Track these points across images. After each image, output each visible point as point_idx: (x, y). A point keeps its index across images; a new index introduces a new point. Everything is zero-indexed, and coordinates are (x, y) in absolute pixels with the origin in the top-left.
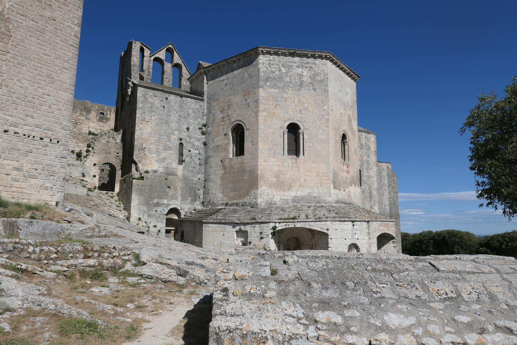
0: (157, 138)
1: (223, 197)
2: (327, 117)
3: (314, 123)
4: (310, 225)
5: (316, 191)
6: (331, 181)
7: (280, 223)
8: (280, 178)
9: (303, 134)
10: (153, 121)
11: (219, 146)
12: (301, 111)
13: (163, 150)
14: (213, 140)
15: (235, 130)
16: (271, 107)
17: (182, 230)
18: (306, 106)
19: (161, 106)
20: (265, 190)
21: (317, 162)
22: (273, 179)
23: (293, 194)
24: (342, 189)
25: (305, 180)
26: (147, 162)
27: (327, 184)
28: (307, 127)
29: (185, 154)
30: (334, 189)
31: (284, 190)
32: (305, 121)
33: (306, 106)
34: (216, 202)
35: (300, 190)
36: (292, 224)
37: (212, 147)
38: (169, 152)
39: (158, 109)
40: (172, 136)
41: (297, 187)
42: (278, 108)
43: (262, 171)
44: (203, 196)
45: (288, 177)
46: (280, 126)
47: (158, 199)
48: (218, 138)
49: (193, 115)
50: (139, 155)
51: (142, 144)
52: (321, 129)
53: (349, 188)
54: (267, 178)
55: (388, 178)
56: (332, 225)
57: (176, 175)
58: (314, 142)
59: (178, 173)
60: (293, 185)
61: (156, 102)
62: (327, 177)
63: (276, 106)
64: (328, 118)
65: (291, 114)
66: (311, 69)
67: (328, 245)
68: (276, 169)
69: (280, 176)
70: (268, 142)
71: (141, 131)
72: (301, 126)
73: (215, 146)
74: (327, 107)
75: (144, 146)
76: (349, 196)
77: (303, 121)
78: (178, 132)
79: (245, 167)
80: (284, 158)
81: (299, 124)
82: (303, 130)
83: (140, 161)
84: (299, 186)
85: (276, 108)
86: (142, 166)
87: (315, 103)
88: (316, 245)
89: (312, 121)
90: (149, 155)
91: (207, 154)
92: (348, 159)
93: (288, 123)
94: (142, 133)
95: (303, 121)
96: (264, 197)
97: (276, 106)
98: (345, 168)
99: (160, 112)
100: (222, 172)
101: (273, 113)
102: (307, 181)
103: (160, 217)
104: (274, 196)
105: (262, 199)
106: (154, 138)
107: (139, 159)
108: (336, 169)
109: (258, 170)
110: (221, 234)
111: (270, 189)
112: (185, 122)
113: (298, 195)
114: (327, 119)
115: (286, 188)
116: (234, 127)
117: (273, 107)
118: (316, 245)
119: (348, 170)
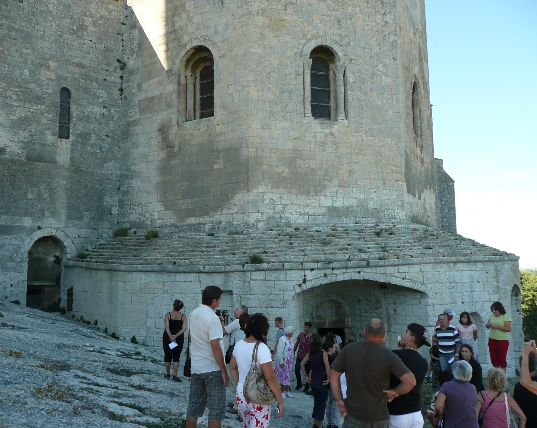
0: (5, 72)
1: (166, 212)
2: (392, 38)
3: (368, 50)
4: (385, 274)
5: (374, 196)
6: (403, 175)
7: (312, 270)
8: (299, 167)
9: (345, 71)
11: (153, 98)
12: (339, 21)
13: (18, 100)
14: (139, 86)
15: (191, 63)
16: (275, 7)
17: (68, 287)
18: (350, 11)
20: (264, 193)
21: (374, 134)
22: (282, 168)
23: (327, 202)
24: (417, 195)
25: (351, 173)
27: (396, 181)
28: (353, 57)
29: (74, 115)
30: (408, 192)
31: (308, 193)
32: (348, 44)
33: (350, 11)
34: (149, 222)
35: (341, 193)
36: (344, 273)
37: (139, 101)
38: (34, 107)
40: (43, 72)
41: (336, 188)
42: (290, 10)
43: (256, 150)
44: (118, 210)
45: (314, 164)
46: (295, 50)
47: (8, 215)
48: (151, 81)
49: (93, 29)
52: (382, 64)
53: (424, 193)
54: (270, 165)
55: (440, 185)
56: (433, 273)
57: (54, 161)
58: (368, 90)
59: (58, 157)
60: (325, 183)
62: (396, 166)
63: (285, 6)
64: (395, 41)
65: (320, 25)
67: (427, 320)
68: (289, 145)
69: (299, 161)
70: (270, 86)
72: (340, 54)
73: (145, 99)
74: (393, 17)
76: (425, 208)
77: (344, 42)
78: (57, 64)
79: (217, 142)
80: (305, 121)
81: (336, 48)
82: (345, 63)
84: (339, 186)
85: (286, 10)
87: (368, 7)
88: (389, 318)
91: (128, 119)
92: (421, 136)
93: (312, 45)
95: (344, 42)
96: (262, 208)
97: (285, 6)
98: (418, 151)
99: (9, 12)
100: (163, 155)
101: (281, 20)
102: (355, 175)
103: (11, 257)
105: (260, 214)
108: (408, 152)
109: (247, 147)
110: (164, 298)
111: (276, 191)
112: (74, 43)
113: (337, 205)
114: (392, 42)
116: (187, 56)
117: (279, 7)
118: (389, 318)
119: (422, 156)
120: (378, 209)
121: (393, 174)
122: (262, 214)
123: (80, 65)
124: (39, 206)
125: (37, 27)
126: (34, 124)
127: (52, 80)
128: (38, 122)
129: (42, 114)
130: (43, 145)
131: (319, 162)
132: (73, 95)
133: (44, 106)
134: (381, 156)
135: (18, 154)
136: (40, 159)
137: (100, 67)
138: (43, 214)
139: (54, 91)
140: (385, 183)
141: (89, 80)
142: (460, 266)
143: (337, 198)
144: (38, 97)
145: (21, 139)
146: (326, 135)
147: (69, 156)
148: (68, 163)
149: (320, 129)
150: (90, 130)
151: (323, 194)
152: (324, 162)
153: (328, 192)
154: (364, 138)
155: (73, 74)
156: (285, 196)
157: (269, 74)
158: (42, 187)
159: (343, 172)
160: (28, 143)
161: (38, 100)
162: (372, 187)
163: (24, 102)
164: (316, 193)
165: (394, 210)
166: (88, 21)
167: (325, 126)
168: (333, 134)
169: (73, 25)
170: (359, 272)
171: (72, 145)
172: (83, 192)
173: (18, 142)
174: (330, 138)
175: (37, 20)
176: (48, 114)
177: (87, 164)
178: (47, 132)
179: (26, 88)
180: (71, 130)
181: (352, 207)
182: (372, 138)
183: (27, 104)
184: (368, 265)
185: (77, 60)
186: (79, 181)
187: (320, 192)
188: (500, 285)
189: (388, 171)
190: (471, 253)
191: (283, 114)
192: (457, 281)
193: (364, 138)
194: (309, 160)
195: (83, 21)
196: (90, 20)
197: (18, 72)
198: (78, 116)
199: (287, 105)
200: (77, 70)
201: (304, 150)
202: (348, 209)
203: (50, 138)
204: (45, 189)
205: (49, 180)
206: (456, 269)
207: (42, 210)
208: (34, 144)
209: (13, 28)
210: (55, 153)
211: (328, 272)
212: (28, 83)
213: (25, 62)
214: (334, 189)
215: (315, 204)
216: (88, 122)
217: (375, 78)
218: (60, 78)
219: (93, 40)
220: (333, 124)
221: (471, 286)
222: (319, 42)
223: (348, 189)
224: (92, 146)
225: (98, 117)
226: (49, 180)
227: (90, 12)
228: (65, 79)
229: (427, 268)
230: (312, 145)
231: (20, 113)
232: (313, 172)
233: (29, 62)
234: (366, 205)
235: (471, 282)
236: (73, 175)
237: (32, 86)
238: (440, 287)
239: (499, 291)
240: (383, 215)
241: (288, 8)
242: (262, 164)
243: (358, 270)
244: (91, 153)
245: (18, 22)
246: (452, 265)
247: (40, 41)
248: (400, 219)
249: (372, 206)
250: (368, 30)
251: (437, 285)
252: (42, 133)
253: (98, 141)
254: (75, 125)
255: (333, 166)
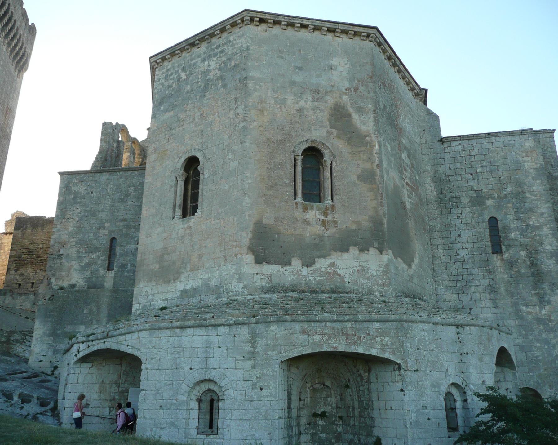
8: (165, 262)
10: (77, 216)
12: (202, 131)
19: (88, 193)
20: (143, 287)
21: (221, 217)
22: (155, 265)
23: (180, 286)
25: (200, 257)
26: (64, 273)
27: (235, 255)
29: (118, 254)
35: (191, 277)
38: (94, 255)
39: (83, 197)
46: (171, 169)
50: (53, 265)
51: (59, 251)
57: (103, 287)
59: (105, 284)
61: (82, 189)
66: (221, 55)
69: (166, 256)
71: (59, 233)
75: (61, 252)
78: (109, 224)
80: (172, 223)
83: (53, 275)
84: (191, 271)
86: (55, 280)
89: (217, 143)
90: (66, 264)
94: (60, 235)
104: (153, 295)
105: (138, 305)
106: (75, 239)
107: (53, 272)
111: (150, 284)
113: (188, 287)
115: (172, 277)
120: (219, 285)
121: (234, 249)
122: (140, 304)
123: (125, 220)
124: (90, 318)
125: (100, 205)
126: (93, 265)
127: (106, 235)
128: (96, 264)
129: (99, 258)
130: (98, 277)
131: (178, 254)
132: (118, 241)
133: (100, 253)
134: (224, 235)
135: (83, 287)
136: (95, 287)
137: (137, 217)
138: (92, 322)
139: (107, 242)
140: (226, 259)
141: (129, 228)
142: (189, 331)
143: (188, 281)
144: (97, 248)
145: (85, 276)
146: (185, 229)
147: (112, 282)
148: (112, 287)
149: (182, 226)
150: (127, 261)
151: (179, 280)
152: (182, 253)
153: (182, 278)
154: (213, 223)
155: (119, 227)
156: (154, 287)
157: (154, 195)
158: (93, 305)
159: (195, 259)
160: (89, 278)
161: (97, 249)
162: (215, 266)
163: (89, 253)
164: (175, 279)
165: (232, 283)
166: (131, 190)
167: (185, 222)
168: (190, 227)
169: (121, 196)
170: (104, 342)
171: (115, 274)
172: (119, 304)
173: (83, 279)
174: (188, 231)
175: (100, 201)
176: (102, 257)
177: (123, 285)
178: (100, 269)
179: (90, 244)
180: (115, 264)
181: (198, 287)
182: (218, 221)
183: (90, 254)
184: (108, 336)
185: (122, 218)
186: (117, 298)
187: (177, 279)
188: (257, 350)
189: (230, 247)
190: (213, 317)
191: (159, 222)
192: (184, 347)
193: (213, 223)
194: (172, 253)
195: (128, 191)
196: (132, 188)
197: (87, 236)
198: (120, 254)
199: (162, 214)
200: (121, 224)
201: (169, 247)
202: (195, 289)
203: (102, 272)
204: (94, 306)
205: (97, 300)
206: (184, 334)
207: (91, 321)
208: (92, 278)
209: (86, 211)
210: (104, 281)
211: (90, 343)
212: (92, 241)
213: (92, 229)
214: (187, 274)
215: (173, 290)
216: (126, 256)
217: (225, 167)
218: (111, 232)
219: (133, 200)
220: (191, 219)
221: (206, 351)
222: (188, 155)
223: (197, 272)
224: (128, 272)
225: (133, 251)
226: (97, 300)
227: (132, 183)
228: (113, 232)
229: (144, 334)
230: (175, 241)
231: (86, 260)
232: (174, 263)
233: (94, 228)
234: (208, 284)
235: (207, 347)
236: (113, 294)
237: (94, 242)
238: (157, 352)
239: (253, 357)
240: (222, 290)
241: (170, 140)
242: (144, 264)
243: (103, 341)
244: (126, 276)
245: (90, 206)
246: (178, 331)
247: (101, 213)
248: (236, 292)
249: (213, 284)
250: (223, 128)
251: (155, 351)
252: (97, 270)
253: (132, 268)
254: (118, 260)
255: (188, 254)
